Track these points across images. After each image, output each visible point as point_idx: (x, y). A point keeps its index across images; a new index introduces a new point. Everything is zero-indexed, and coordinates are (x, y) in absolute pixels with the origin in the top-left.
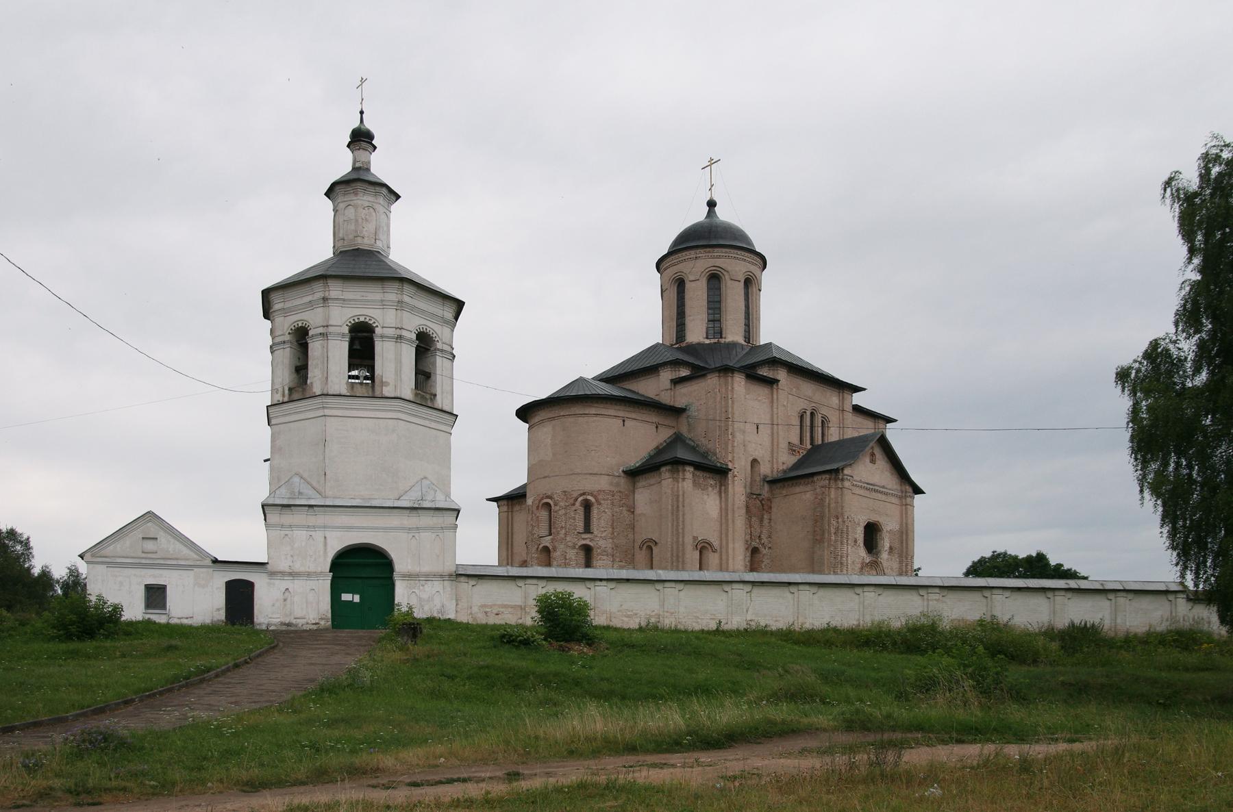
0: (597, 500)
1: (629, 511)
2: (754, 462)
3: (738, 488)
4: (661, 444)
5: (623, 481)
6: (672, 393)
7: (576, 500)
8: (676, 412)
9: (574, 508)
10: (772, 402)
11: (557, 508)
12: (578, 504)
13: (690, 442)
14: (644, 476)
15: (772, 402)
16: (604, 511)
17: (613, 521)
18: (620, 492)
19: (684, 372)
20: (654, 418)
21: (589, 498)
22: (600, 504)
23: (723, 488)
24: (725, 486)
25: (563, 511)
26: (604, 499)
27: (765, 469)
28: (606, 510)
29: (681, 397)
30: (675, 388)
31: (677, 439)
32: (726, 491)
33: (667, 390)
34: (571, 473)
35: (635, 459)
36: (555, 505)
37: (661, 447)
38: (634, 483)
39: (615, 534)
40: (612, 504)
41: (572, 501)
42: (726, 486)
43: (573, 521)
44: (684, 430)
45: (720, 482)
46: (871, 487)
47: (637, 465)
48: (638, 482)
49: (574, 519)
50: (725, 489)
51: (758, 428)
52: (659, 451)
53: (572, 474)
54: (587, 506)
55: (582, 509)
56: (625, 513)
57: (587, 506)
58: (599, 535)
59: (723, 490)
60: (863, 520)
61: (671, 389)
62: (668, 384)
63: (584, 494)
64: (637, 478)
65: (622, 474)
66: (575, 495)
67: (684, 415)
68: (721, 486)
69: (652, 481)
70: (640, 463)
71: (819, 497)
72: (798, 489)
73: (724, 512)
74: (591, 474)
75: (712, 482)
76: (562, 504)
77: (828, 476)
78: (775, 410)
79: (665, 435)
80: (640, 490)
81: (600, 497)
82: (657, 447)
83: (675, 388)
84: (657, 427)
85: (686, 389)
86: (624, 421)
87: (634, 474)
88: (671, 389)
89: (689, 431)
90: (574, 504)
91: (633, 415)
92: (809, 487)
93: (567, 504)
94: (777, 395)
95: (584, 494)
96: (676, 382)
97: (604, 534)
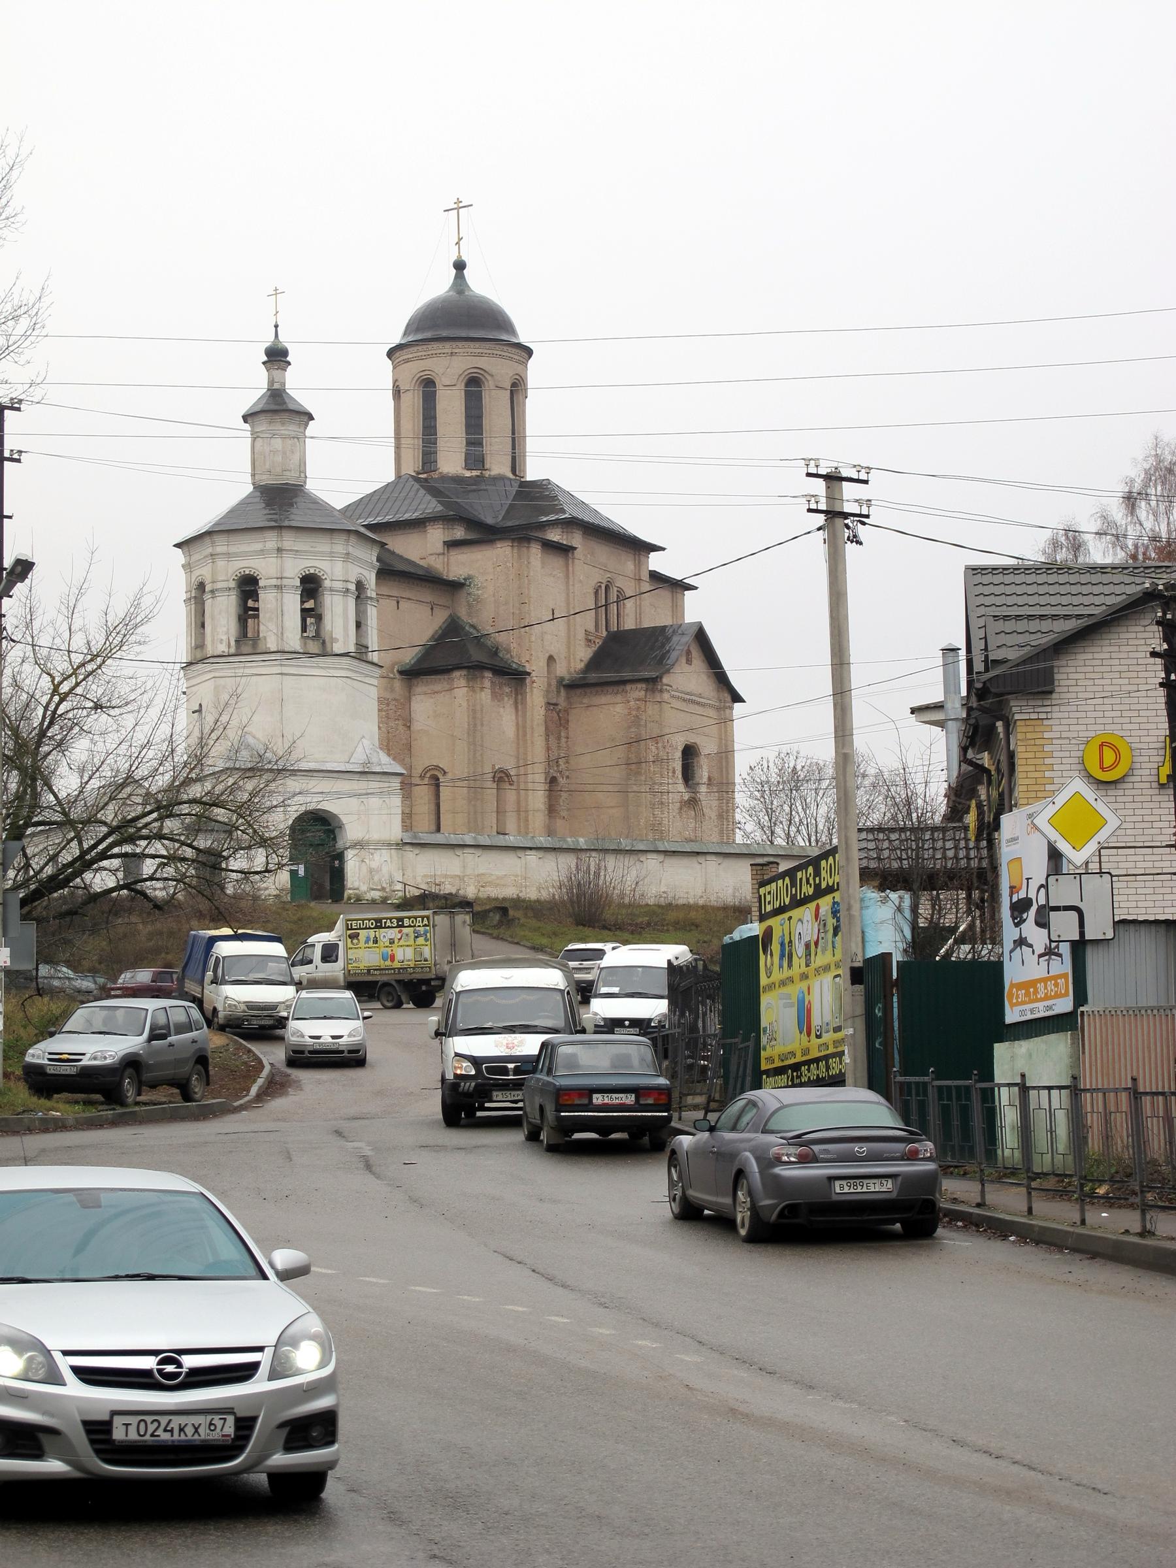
2: (551, 659)
3: (536, 696)
5: (398, 684)
6: (446, 560)
8: (455, 587)
10: (567, 576)
15: (567, 576)
23: (520, 697)
24: (521, 694)
29: (459, 565)
30: (448, 552)
31: (453, 627)
32: (524, 702)
33: (439, 555)
38: (410, 688)
42: (524, 694)
45: (516, 690)
48: (417, 686)
50: (522, 699)
56: (401, 728)
59: (519, 701)
61: (443, 554)
62: (439, 547)
64: (415, 681)
65: (398, 676)
67: (462, 594)
68: (517, 694)
69: (437, 687)
70: (415, 659)
71: (634, 713)
72: (603, 699)
73: (522, 730)
75: (507, 690)
77: (644, 686)
78: (571, 587)
79: (439, 619)
84: (432, 609)
85: (465, 556)
89: (469, 615)
92: (619, 698)
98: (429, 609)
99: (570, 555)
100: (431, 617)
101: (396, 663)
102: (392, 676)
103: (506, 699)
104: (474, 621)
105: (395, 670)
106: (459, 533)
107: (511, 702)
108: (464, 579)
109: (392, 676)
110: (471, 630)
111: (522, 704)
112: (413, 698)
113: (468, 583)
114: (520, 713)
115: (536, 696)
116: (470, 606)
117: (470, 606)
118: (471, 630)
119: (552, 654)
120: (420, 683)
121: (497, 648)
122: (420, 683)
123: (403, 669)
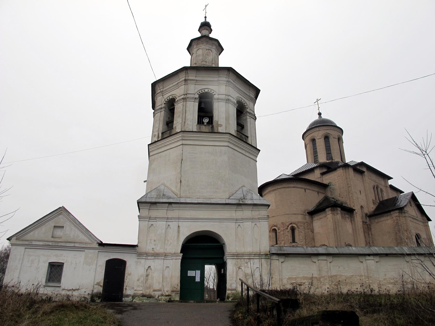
0: (297, 227)
1: (311, 231)
2: (362, 207)
3: (358, 217)
4: (320, 201)
5: (307, 217)
6: (322, 179)
7: (288, 226)
8: (324, 186)
9: (287, 230)
10: (363, 181)
11: (280, 231)
12: (289, 228)
13: (334, 200)
14: (317, 215)
15: (363, 181)
16: (301, 232)
17: (305, 236)
18: (307, 222)
19: (325, 170)
20: (316, 189)
21: (294, 225)
22: (299, 228)
23: (352, 219)
24: (353, 218)
25: (282, 232)
26: (301, 226)
27: (366, 211)
28: (302, 231)
29: (326, 180)
30: (322, 177)
31: (326, 199)
32: (354, 220)
33: (319, 178)
34: (285, 214)
35: (311, 208)
36: (279, 229)
37: (321, 202)
38: (312, 218)
39: (307, 243)
40: (304, 228)
41: (286, 227)
42: (354, 218)
43: (287, 237)
44: (329, 195)
45: (351, 216)
46: (414, 217)
47: (312, 210)
48: (314, 217)
49: (288, 236)
50: (353, 219)
51: (360, 192)
52: (320, 204)
53: (285, 214)
54: (293, 229)
55: (291, 231)
56: (310, 232)
57: (293, 229)
58: (300, 244)
59: (352, 220)
60: (414, 232)
61: (321, 177)
62: (319, 175)
63: (291, 224)
64: (313, 216)
65: (307, 214)
66: (288, 224)
67: (328, 188)
68: (351, 218)
69: (321, 216)
70: (313, 209)
72: (383, 219)
74: (293, 214)
75: (347, 216)
76: (282, 229)
78: (365, 185)
79: (321, 197)
80: (315, 221)
81: (299, 225)
82: (319, 202)
83: (322, 177)
84: (318, 193)
86: (305, 190)
87: (312, 214)
88: (321, 177)
89: (331, 195)
90: (287, 229)
91: (308, 188)
92: (389, 217)
93: (284, 229)
94: (365, 178)
95: (291, 224)
96: (323, 174)
97: (302, 243)
98: (317, 193)
99: (363, 174)
100: (318, 196)
101: (307, 210)
102: (305, 214)
103: (347, 219)
104: (333, 196)
105: (306, 212)
106: (325, 170)
107: (350, 220)
108: (329, 184)
109: (305, 214)
110: (333, 199)
111: (353, 221)
112: (314, 222)
113: (329, 185)
114: (353, 224)
115: (358, 217)
116: (331, 192)
117: (331, 192)
118: (333, 199)
119: (362, 205)
120: (315, 216)
121: (342, 203)
122: (315, 216)
123: (309, 212)
